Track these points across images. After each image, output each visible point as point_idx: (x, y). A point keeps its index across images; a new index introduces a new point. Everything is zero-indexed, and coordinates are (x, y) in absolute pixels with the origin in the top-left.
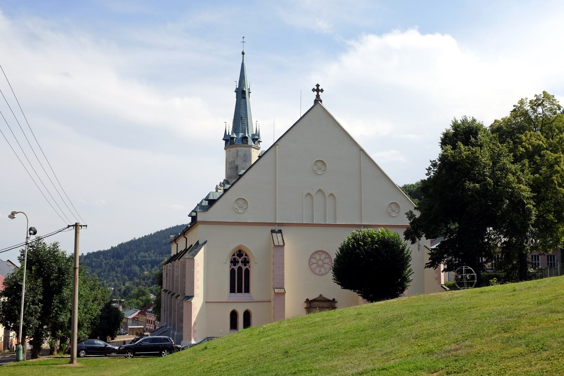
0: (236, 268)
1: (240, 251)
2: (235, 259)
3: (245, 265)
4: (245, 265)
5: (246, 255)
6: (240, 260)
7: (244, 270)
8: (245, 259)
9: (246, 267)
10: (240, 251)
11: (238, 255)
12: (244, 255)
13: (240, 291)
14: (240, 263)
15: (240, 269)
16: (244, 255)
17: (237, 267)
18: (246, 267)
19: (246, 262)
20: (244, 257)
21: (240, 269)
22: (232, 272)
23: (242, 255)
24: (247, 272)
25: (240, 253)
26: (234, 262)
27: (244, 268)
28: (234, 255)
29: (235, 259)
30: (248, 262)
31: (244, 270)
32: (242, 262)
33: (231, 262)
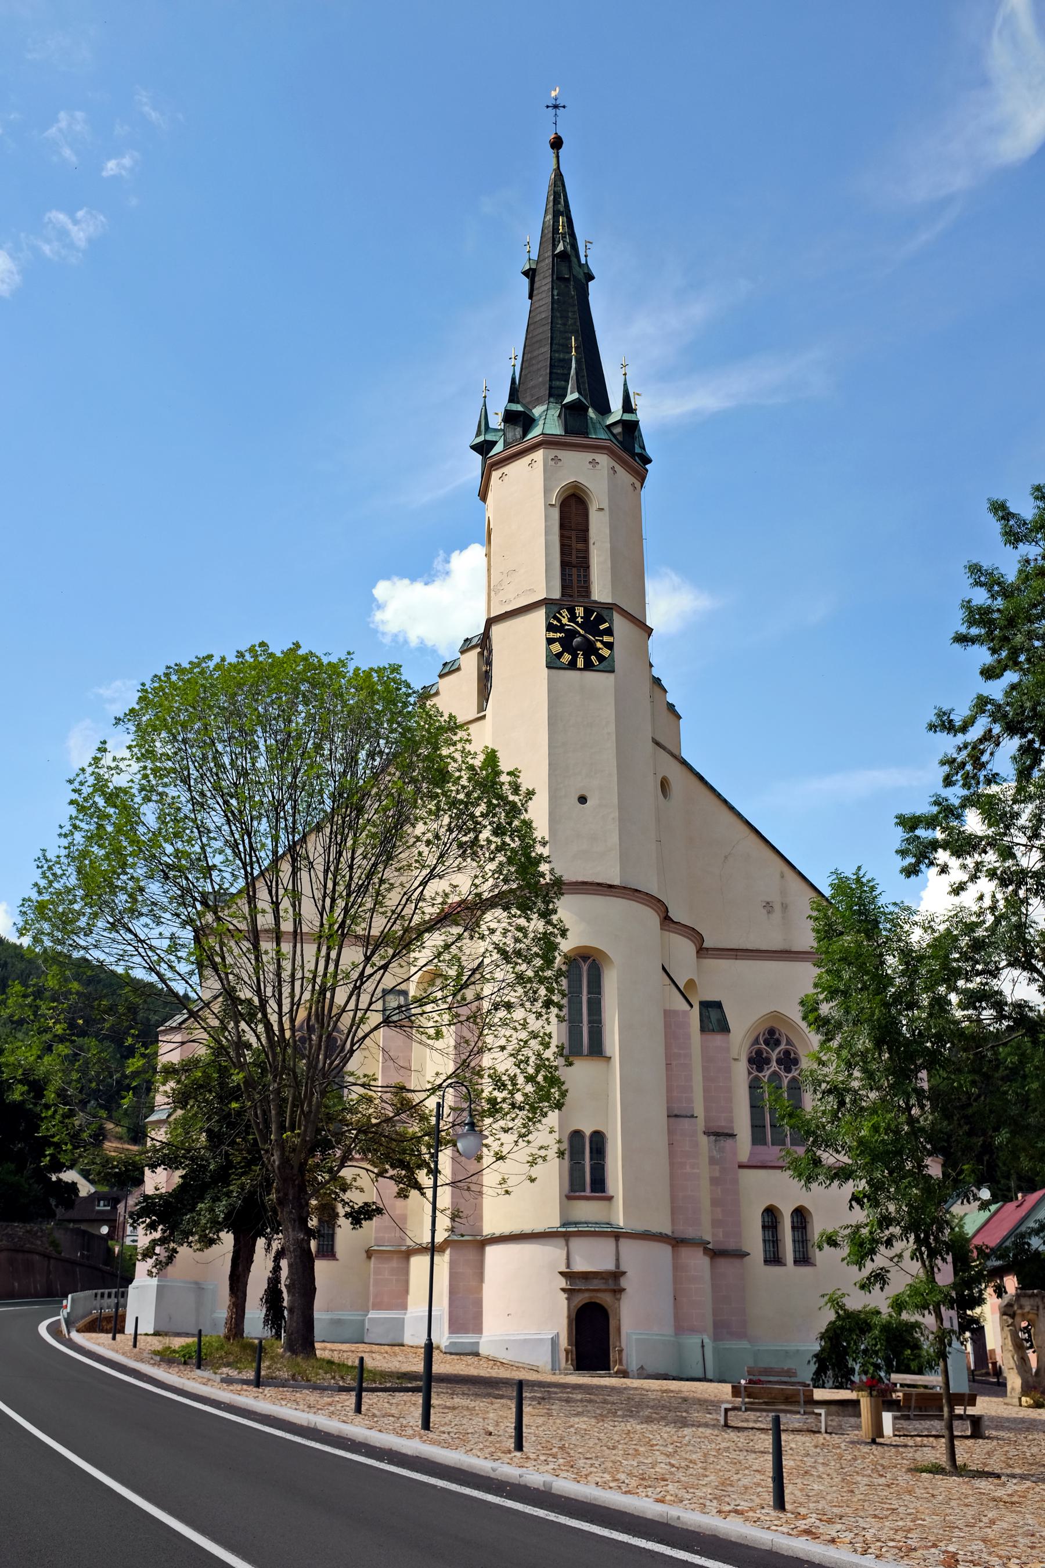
1: (772, 1032)
2: (759, 1052)
3: (788, 1070)
4: (788, 1070)
5: (789, 1042)
6: (774, 1056)
8: (787, 1053)
9: (790, 1075)
10: (772, 1032)
11: (767, 1043)
12: (784, 1042)
14: (775, 1064)
16: (784, 1042)
18: (790, 1075)
20: (783, 1046)
22: (754, 1086)
23: (778, 1043)
26: (758, 1061)
28: (756, 1041)
29: (759, 1052)
31: (786, 1082)
32: (779, 1062)
33: (751, 1061)
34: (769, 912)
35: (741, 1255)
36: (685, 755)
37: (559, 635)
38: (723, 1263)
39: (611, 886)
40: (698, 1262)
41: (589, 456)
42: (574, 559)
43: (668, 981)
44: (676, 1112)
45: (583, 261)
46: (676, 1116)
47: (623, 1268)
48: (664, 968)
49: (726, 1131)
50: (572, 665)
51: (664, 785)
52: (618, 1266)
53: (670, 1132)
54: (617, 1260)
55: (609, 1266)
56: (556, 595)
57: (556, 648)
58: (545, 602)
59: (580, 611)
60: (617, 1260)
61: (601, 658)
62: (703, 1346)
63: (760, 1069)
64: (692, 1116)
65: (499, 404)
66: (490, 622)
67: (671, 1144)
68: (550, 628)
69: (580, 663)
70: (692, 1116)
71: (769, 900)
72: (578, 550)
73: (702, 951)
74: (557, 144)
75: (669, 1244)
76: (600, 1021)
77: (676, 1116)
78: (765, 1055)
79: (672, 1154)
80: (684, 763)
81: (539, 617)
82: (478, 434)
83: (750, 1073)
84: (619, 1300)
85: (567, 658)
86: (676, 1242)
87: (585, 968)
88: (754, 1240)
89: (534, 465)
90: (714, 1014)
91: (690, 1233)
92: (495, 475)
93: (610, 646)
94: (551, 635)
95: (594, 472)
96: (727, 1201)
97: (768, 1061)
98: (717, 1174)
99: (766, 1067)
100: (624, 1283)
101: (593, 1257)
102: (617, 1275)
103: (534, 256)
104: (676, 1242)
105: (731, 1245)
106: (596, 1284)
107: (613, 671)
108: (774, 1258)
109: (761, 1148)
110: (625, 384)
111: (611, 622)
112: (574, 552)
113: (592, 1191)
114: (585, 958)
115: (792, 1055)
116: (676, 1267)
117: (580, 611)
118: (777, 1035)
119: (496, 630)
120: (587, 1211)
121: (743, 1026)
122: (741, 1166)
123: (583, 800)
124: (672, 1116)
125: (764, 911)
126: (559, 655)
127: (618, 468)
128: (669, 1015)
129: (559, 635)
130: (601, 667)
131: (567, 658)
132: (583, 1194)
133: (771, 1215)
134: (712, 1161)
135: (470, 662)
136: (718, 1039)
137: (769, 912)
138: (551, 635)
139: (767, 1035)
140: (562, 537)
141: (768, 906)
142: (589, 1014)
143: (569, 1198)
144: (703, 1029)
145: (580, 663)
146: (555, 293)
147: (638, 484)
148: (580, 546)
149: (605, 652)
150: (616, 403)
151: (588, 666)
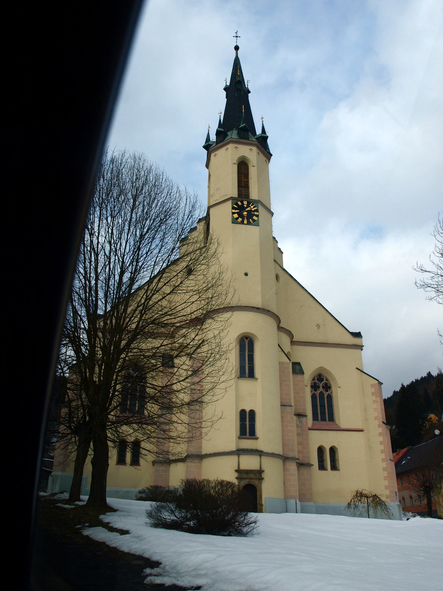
0: (317, 393)
2: (315, 383)
5: (327, 380)
6: (321, 385)
7: (326, 396)
8: (326, 384)
9: (328, 393)
11: (318, 379)
12: (325, 380)
13: (323, 419)
14: (321, 388)
15: (321, 394)
16: (325, 380)
18: (328, 393)
19: (327, 387)
20: (324, 381)
21: (321, 394)
22: (314, 397)
23: (322, 380)
24: (330, 397)
26: (314, 387)
28: (314, 379)
29: (315, 383)
31: (326, 395)
32: (323, 387)
33: (312, 387)
34: (318, 328)
35: (310, 465)
36: (285, 267)
37: (237, 211)
38: (303, 469)
39: (258, 308)
40: (292, 467)
41: (250, 147)
42: (243, 184)
43: (280, 350)
44: (284, 404)
45: (246, 87)
46: (284, 405)
47: (263, 469)
48: (279, 345)
49: (303, 414)
50: (242, 222)
51: (277, 277)
52: (261, 468)
53: (282, 412)
54: (261, 465)
55: (257, 467)
56: (235, 195)
57: (236, 216)
58: (232, 198)
59: (245, 203)
60: (261, 465)
61: (254, 221)
62: (296, 504)
64: (291, 406)
65: (214, 127)
66: (209, 208)
67: (282, 417)
68: (233, 208)
69: (245, 222)
70: (291, 406)
71: (318, 323)
72: (244, 182)
73: (293, 343)
74: (237, 48)
75: (281, 459)
76: (253, 364)
77: (284, 405)
78: (317, 384)
79: (282, 422)
80: (284, 270)
81: (229, 204)
82: (206, 143)
83: (311, 392)
84: (261, 483)
85: (240, 219)
86: (285, 458)
87: (247, 342)
88: (314, 460)
89: (228, 150)
90: (297, 367)
91: (291, 454)
92: (212, 155)
93: (257, 216)
94: (234, 211)
95: (250, 153)
96: (303, 443)
97: (319, 387)
98: (300, 432)
99: (318, 389)
100: (263, 475)
101: (249, 463)
102: (260, 472)
103: (228, 84)
104: (285, 458)
105: (306, 461)
106: (252, 476)
107: (259, 226)
108: (322, 467)
109: (316, 422)
110: (263, 124)
111: (258, 207)
112: (243, 182)
113: (250, 435)
114: (247, 338)
115: (328, 385)
116: (284, 470)
117: (245, 203)
118: (322, 377)
119: (212, 210)
120: (247, 444)
121: (309, 371)
122: (310, 429)
123: (246, 274)
124: (283, 405)
125: (317, 328)
126: (237, 219)
127: (260, 153)
128: (281, 364)
129: (237, 211)
130: (254, 224)
131: (240, 219)
132: (245, 436)
133: (321, 450)
134: (298, 426)
135: (201, 227)
136: (299, 377)
137: (318, 328)
138: (234, 211)
139: (318, 377)
140: (238, 176)
141: (318, 326)
142: (249, 361)
143: (239, 438)
144: (293, 373)
145: (245, 222)
146: (236, 94)
147: (267, 161)
148: (245, 180)
149: (255, 218)
150: (259, 131)
151: (249, 223)
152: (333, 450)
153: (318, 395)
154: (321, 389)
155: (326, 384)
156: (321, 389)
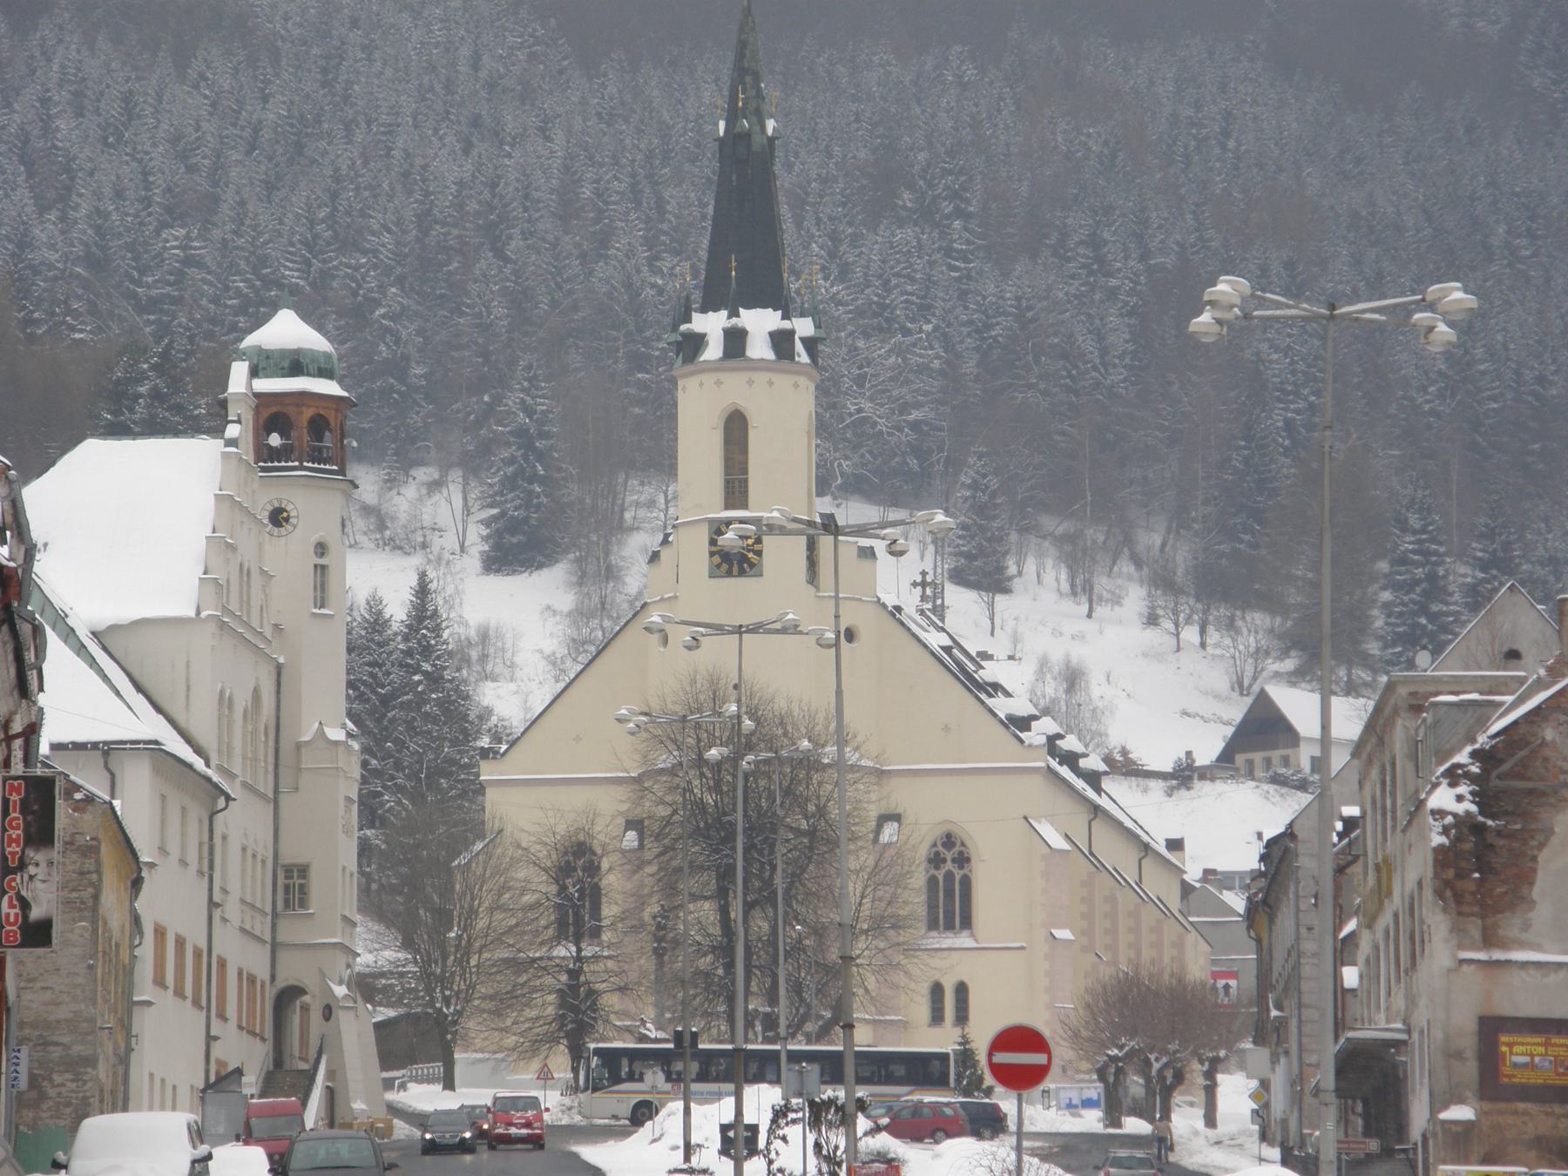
2: (937, 854)
3: (961, 867)
4: (961, 867)
5: (963, 844)
6: (949, 856)
8: (961, 853)
10: (949, 836)
11: (944, 845)
13: (949, 927)
15: (949, 876)
17: (943, 871)
19: (963, 860)
20: (957, 848)
21: (949, 876)
22: (932, 881)
23: (953, 845)
24: (966, 883)
25: (949, 840)
26: (936, 860)
27: (958, 874)
28: (935, 845)
29: (937, 854)
30: (968, 860)
32: (954, 860)
33: (930, 861)
50: (729, 574)
61: (752, 565)
63: (937, 868)
85: (725, 567)
97: (944, 861)
126: (718, 566)
131: (725, 567)
133: (937, 990)
145: (735, 569)
151: (742, 573)
152: (962, 990)
153: (941, 879)
154: (949, 865)
155: (961, 853)
156: (949, 865)
